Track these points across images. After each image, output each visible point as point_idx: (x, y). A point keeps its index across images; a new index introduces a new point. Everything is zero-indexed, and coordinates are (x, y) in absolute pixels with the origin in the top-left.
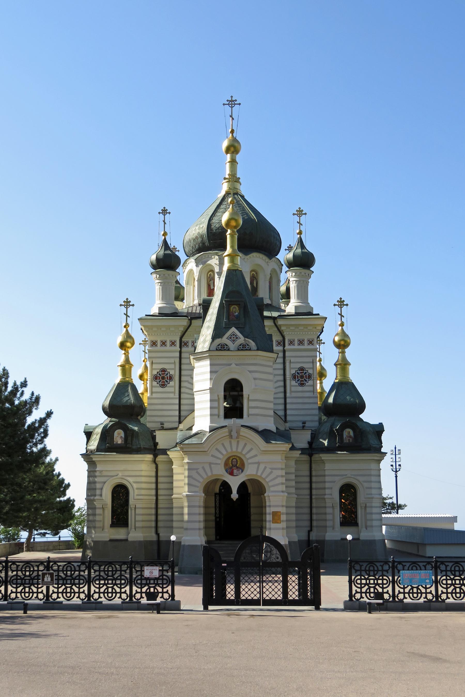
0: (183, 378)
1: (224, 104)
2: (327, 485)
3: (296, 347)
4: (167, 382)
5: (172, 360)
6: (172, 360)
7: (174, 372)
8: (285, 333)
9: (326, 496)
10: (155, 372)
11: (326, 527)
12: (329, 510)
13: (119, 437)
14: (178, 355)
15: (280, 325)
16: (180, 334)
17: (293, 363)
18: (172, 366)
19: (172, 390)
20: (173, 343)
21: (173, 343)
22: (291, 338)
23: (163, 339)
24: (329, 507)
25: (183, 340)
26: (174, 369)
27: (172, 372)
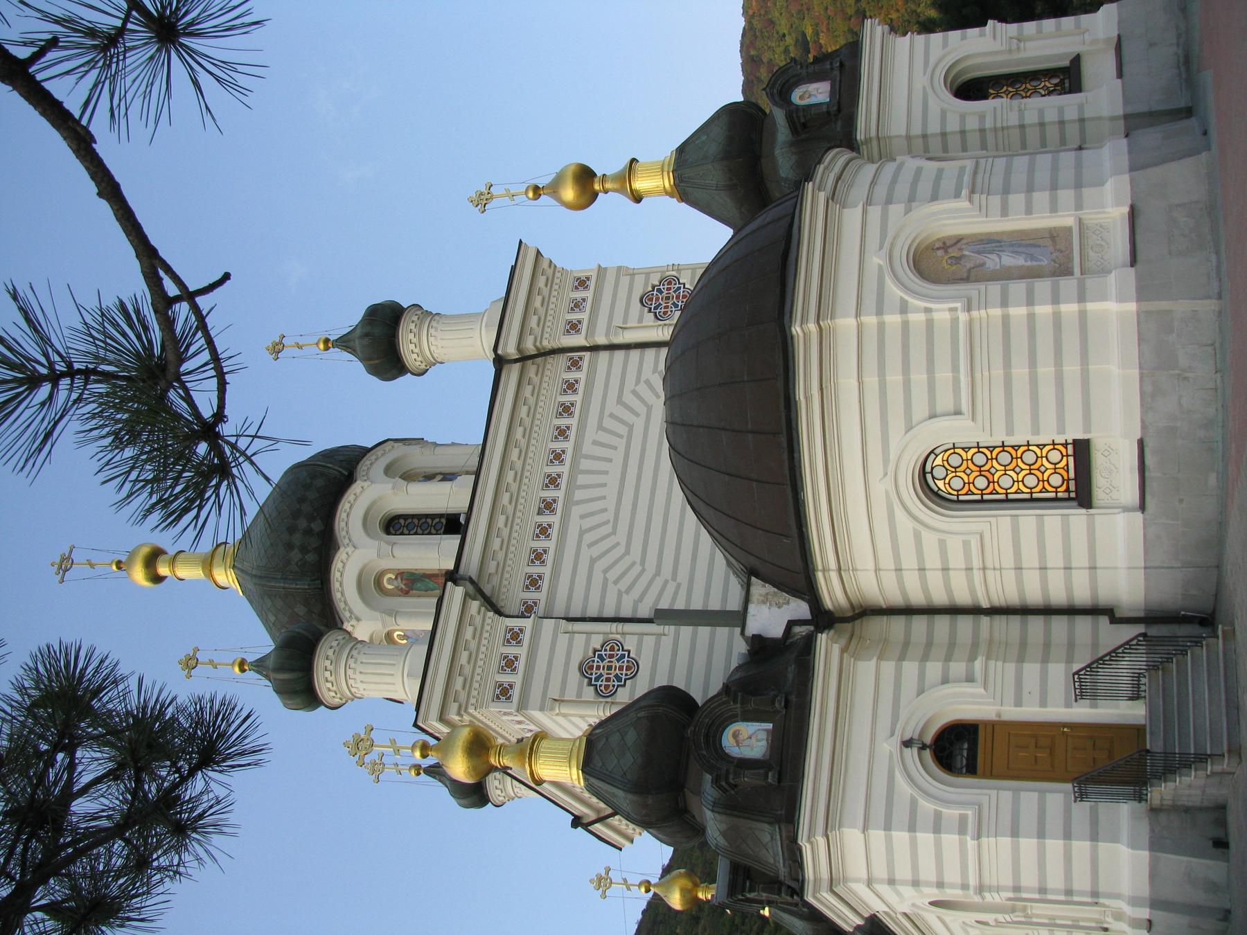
0: (626, 612)
1: (62, 581)
2: (953, 125)
3: (584, 316)
4: (623, 656)
5: (563, 640)
6: (563, 640)
7: (598, 634)
8: (545, 343)
9: (989, 124)
10: (589, 692)
11: (1082, 121)
12: (1031, 118)
13: (748, 739)
14: (548, 624)
15: (519, 349)
16: (491, 614)
17: (625, 321)
18: (579, 640)
19: (649, 641)
20: (515, 636)
21: (515, 636)
22: (562, 326)
23: (495, 662)
24: (1021, 116)
25: (514, 607)
26: (589, 634)
27: (596, 642)
